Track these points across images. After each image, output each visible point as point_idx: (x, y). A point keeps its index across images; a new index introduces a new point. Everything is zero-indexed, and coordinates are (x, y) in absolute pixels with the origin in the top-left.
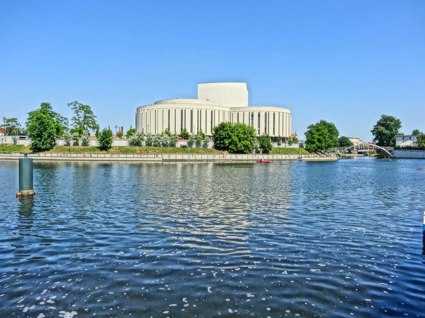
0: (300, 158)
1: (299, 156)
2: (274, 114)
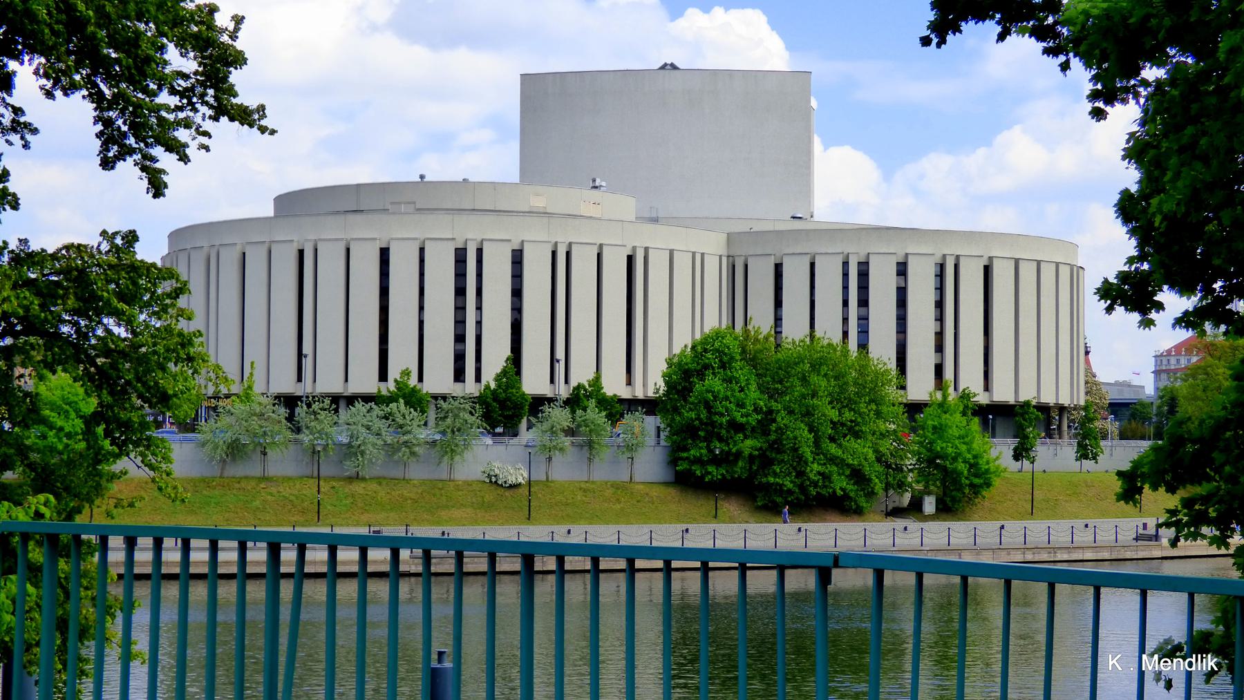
0: (1149, 538)
1: (1145, 526)
2: (987, 270)
